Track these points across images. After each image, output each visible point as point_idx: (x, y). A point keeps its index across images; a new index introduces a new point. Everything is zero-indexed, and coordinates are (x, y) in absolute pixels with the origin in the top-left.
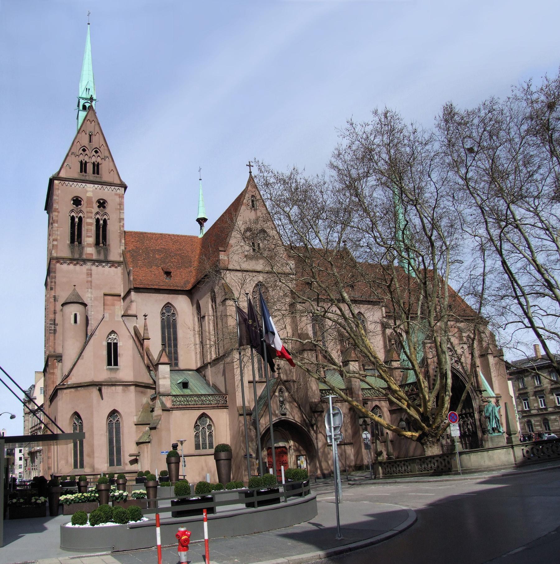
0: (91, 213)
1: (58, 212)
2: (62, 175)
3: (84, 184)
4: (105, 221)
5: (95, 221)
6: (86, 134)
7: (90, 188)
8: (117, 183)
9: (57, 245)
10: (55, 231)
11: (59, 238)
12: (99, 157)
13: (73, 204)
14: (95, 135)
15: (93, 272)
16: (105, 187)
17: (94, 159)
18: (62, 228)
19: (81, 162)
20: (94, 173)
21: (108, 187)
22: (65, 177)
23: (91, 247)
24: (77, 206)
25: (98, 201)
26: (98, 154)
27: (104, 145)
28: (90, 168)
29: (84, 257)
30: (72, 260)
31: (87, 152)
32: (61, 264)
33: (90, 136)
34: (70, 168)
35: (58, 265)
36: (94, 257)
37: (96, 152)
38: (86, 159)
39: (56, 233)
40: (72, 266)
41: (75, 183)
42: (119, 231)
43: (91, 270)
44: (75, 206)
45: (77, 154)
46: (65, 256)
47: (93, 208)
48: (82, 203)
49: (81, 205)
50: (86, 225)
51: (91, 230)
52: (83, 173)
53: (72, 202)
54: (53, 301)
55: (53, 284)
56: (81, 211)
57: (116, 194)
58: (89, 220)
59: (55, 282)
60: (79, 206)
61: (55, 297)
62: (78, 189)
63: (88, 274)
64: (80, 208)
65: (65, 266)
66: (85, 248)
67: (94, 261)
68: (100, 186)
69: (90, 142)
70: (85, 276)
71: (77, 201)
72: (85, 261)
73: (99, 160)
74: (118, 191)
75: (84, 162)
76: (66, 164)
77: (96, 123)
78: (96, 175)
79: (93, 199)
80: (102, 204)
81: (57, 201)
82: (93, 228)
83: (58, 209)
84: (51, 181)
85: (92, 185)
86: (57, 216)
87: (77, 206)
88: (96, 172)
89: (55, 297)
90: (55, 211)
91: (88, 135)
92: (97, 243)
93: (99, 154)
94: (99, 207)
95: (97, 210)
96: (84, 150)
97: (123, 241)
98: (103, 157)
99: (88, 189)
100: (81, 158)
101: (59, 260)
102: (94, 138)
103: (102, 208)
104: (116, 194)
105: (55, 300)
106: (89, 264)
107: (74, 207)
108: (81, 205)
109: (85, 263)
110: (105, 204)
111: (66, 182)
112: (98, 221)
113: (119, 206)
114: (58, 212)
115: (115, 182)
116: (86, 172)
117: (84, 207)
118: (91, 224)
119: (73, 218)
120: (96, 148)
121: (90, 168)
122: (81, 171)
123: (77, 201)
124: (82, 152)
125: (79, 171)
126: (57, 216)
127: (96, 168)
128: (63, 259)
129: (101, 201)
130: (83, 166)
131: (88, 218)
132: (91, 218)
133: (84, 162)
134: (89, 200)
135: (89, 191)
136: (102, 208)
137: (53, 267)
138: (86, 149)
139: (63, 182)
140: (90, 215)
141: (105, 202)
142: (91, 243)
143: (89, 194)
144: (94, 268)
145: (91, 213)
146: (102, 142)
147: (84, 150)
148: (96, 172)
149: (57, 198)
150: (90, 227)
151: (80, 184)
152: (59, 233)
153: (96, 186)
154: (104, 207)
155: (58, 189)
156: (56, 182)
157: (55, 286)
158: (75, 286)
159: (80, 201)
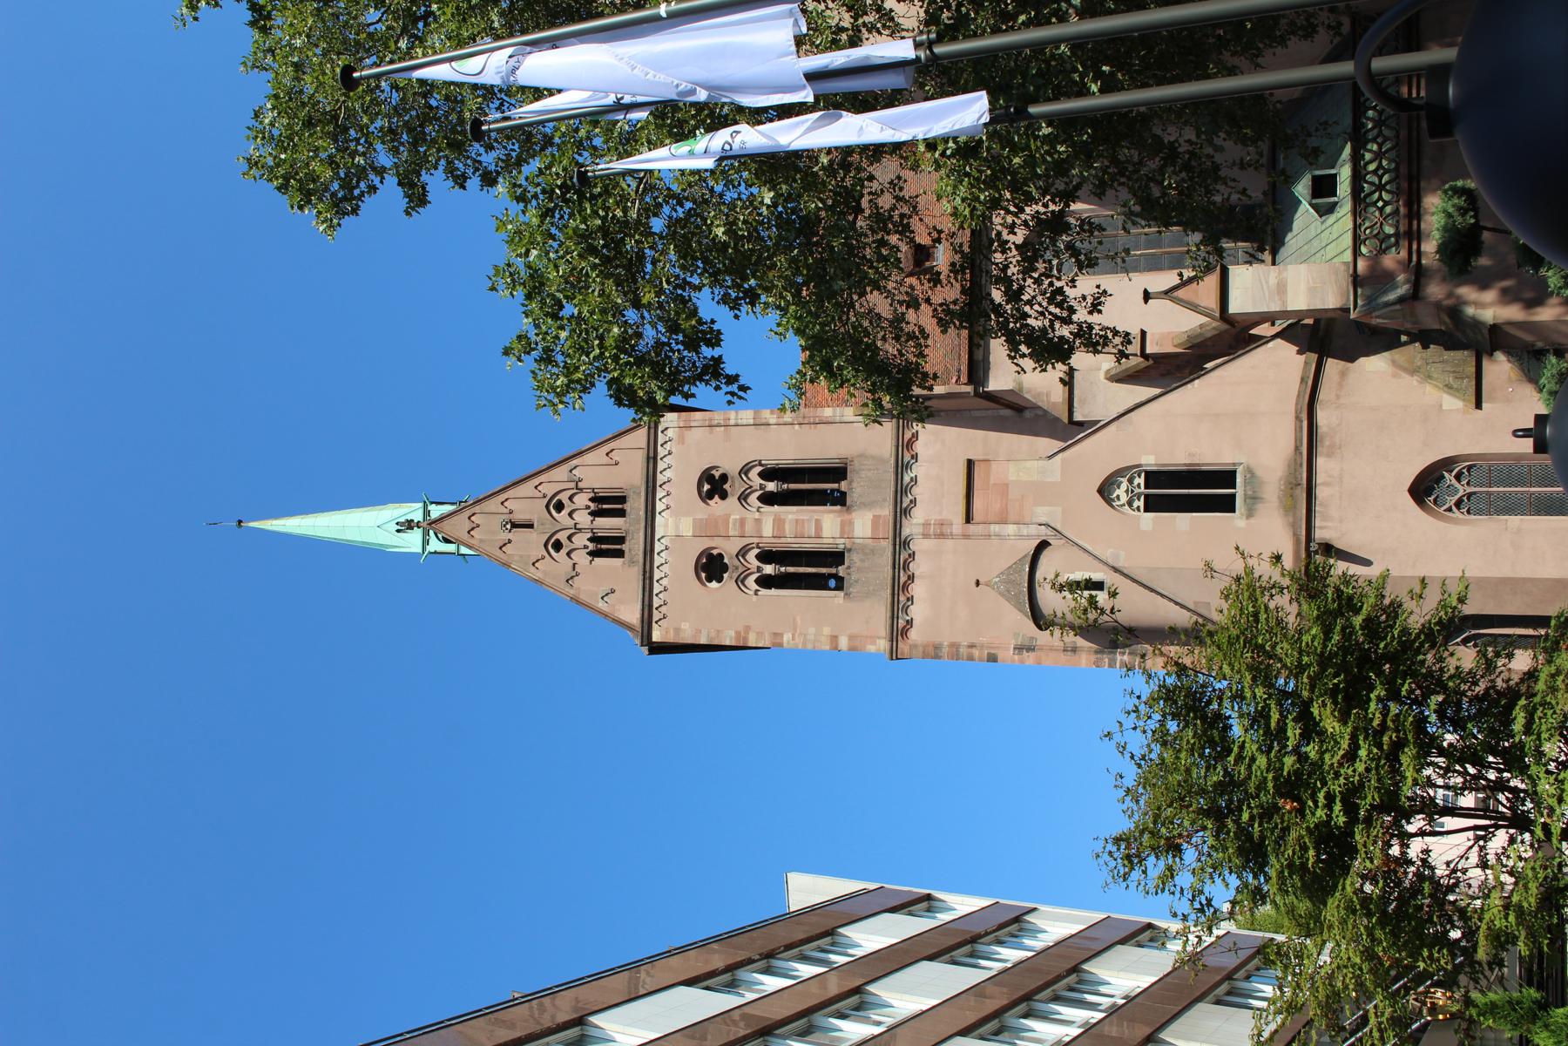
0: (742, 522)
1: (748, 629)
2: (632, 615)
3: (658, 547)
4: (768, 474)
5: (766, 509)
6: (510, 541)
7: (666, 526)
8: (645, 439)
9: (851, 638)
10: (804, 643)
11: (827, 631)
12: (575, 499)
13: (720, 580)
14: (511, 512)
15: (934, 518)
16: (660, 478)
17: (583, 518)
18: (794, 620)
19: (594, 554)
20: (621, 513)
21: (661, 465)
22: (639, 606)
23: (851, 523)
24: (725, 568)
25: (707, 497)
26: (566, 501)
27: (536, 481)
28: (607, 524)
29: (887, 545)
30: (900, 589)
31: (562, 536)
32: (910, 623)
33: (515, 525)
34: (613, 591)
35: (913, 634)
36: (887, 511)
37: (560, 507)
38: (581, 540)
39: (812, 637)
40: (917, 589)
41: (657, 574)
42: (797, 427)
43: (926, 524)
44: (725, 575)
45: (571, 568)
46: (883, 609)
47: (726, 518)
48: (715, 552)
49: (721, 556)
50: (783, 540)
51: (797, 521)
52: (624, 547)
53: (714, 584)
54: (1031, 654)
55: (976, 653)
56: (743, 552)
57: (682, 440)
58: (768, 530)
59: (972, 646)
60: (726, 561)
61: (1019, 649)
62: (675, 566)
63: (941, 536)
64: (731, 558)
65: (917, 612)
66: (858, 541)
67: (901, 512)
68: (660, 493)
69: (531, 526)
70: (949, 543)
71: (712, 567)
72: (900, 543)
73: (582, 500)
74: (670, 433)
75: (591, 546)
76: (601, 605)
77: (477, 509)
78: (627, 507)
79: (699, 516)
80: (713, 485)
81: (713, 634)
82: (791, 513)
83: (738, 633)
84: (657, 649)
85: (658, 518)
86: (760, 634)
87: (725, 568)
88: (620, 506)
89: (1019, 649)
90: (745, 639)
91: (510, 536)
92: (840, 499)
93: (564, 497)
94: (724, 496)
95: (732, 501)
96: (558, 546)
97: (828, 412)
98: (572, 485)
99: (671, 532)
100: (581, 558)
101: (898, 631)
102: (519, 517)
103: (726, 487)
104: (682, 440)
105: (1030, 649)
106: (906, 532)
107: (731, 577)
108: (721, 556)
109: (906, 544)
110: (713, 476)
111: (655, 605)
112: (768, 499)
113: (718, 429)
114: (748, 629)
115: (644, 445)
116: (621, 540)
117: (728, 548)
118: (779, 522)
119: (765, 582)
120: (547, 507)
121: (607, 524)
122: (619, 554)
123: (712, 567)
124: (564, 551)
125: (617, 562)
126: (760, 634)
127: (608, 504)
128: (894, 617)
129: (706, 487)
130: (607, 547)
131: (759, 529)
132: (758, 521)
133: (591, 546)
134: (703, 529)
135: (677, 527)
136: (726, 487)
137: (921, 649)
138: (553, 541)
139: (656, 615)
140: (749, 529)
141: (707, 476)
142: (839, 520)
143: (686, 527)
144: (918, 516)
145: (742, 522)
146: (527, 489)
147: (558, 546)
148: (620, 506)
149: (704, 633)
150: (787, 527)
151: (658, 561)
152: (812, 630)
153: (659, 506)
154: (724, 478)
155: (677, 630)
156: (657, 636)
157: (982, 646)
158: (978, 583)
159: (711, 557)
